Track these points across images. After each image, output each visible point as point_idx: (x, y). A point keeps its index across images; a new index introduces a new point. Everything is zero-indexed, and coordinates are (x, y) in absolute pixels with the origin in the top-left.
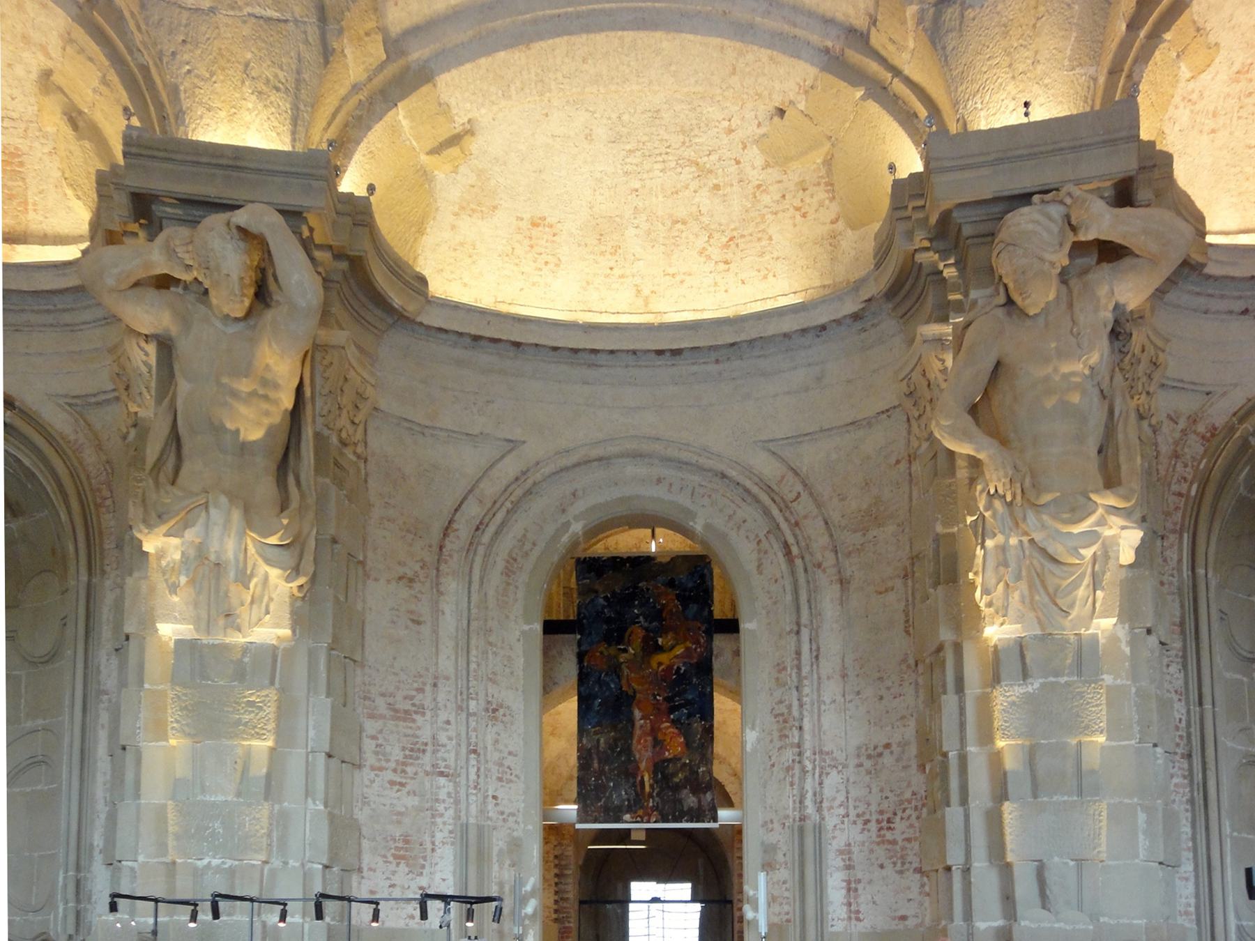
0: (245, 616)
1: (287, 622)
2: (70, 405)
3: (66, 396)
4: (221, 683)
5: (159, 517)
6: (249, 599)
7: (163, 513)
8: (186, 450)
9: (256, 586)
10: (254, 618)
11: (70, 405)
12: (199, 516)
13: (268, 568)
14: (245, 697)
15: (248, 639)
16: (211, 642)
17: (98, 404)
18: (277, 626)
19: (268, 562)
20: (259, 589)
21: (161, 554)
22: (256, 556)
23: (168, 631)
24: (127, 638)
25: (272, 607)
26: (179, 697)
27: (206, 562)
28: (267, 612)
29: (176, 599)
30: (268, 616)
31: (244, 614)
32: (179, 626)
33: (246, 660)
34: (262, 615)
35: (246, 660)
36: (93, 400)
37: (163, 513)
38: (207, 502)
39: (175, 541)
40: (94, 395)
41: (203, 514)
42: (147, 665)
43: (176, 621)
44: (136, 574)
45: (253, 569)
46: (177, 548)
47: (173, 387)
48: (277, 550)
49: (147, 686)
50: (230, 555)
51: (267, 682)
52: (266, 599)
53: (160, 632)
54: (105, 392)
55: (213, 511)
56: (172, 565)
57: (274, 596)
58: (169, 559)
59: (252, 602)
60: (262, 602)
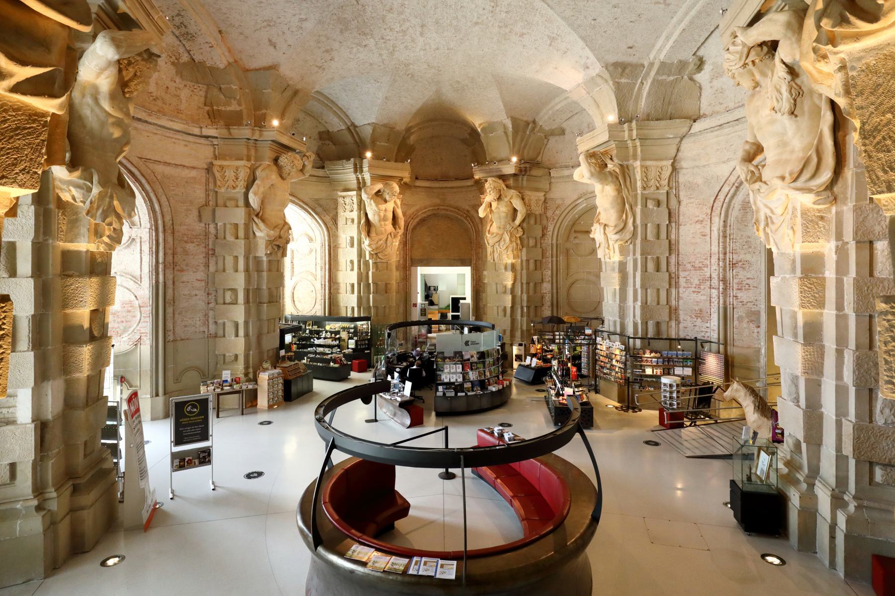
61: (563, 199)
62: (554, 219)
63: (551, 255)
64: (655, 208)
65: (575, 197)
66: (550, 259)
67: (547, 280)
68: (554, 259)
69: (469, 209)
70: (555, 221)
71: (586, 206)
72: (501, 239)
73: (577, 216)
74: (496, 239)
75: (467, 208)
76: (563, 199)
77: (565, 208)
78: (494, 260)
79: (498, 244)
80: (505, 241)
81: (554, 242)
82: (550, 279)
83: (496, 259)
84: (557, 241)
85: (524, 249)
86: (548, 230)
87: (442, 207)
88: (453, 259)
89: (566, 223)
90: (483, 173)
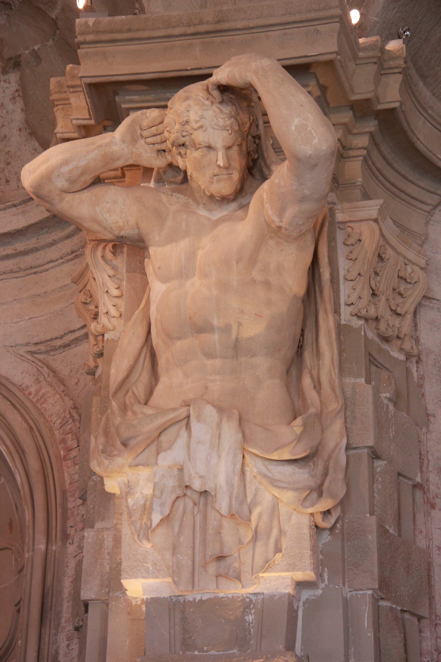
0: (247, 558)
1: (308, 561)
2: (32, 353)
3: (27, 344)
4: (213, 652)
5: (125, 444)
6: (250, 535)
7: (130, 438)
8: (162, 362)
9: (260, 516)
10: (259, 560)
11: (32, 353)
12: (177, 436)
13: (276, 492)
15: (252, 589)
16: (198, 598)
17: (66, 346)
18: (292, 567)
19: (273, 482)
20: (265, 518)
24: (86, 605)
25: (284, 544)
27: (189, 493)
28: (278, 550)
29: (147, 545)
30: (279, 556)
32: (151, 581)
33: (250, 618)
34: (271, 555)
35: (250, 618)
36: (59, 343)
37: (130, 438)
38: (188, 417)
40: (61, 337)
41: (184, 433)
42: (109, 640)
43: (147, 574)
44: (98, 525)
45: (255, 495)
47: (146, 296)
48: (288, 469)
50: (222, 480)
51: (281, 647)
52: (275, 532)
53: (130, 593)
54: (72, 332)
55: (194, 424)
56: (142, 502)
57: (286, 527)
58: (138, 495)
59: (255, 538)
60: (268, 537)
64: (391, 407)
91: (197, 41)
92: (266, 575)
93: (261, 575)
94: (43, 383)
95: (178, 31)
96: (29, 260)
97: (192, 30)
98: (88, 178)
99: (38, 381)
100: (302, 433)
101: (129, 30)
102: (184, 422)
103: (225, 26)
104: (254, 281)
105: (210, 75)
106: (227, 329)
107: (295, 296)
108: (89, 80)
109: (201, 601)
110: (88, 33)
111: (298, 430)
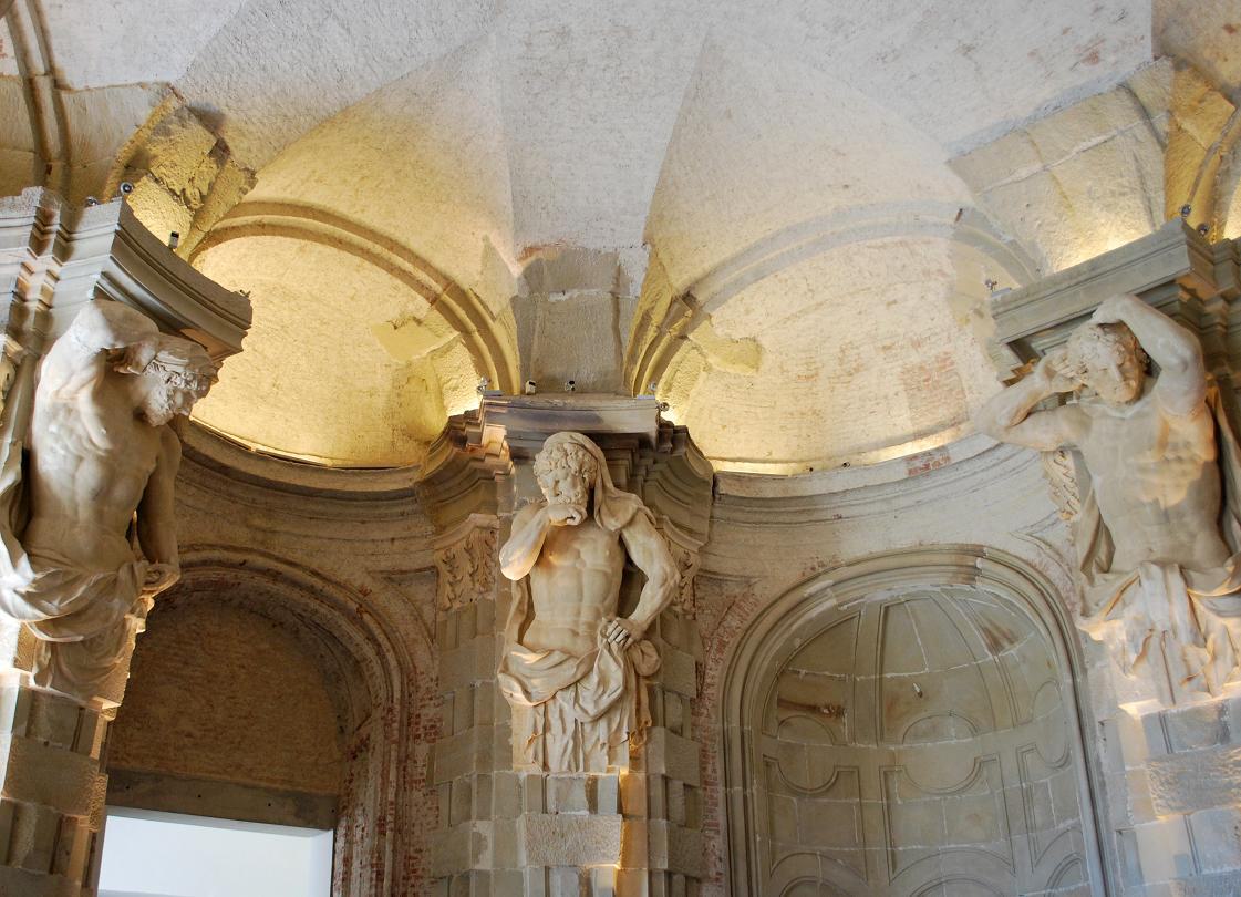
0: (1212, 675)
3: (1026, 527)
4: (1201, 749)
14: (1231, 757)
15: (1221, 697)
19: (1220, 613)
21: (1110, 637)
22: (1207, 612)
23: (1134, 709)
26: (1157, 773)
31: (1216, 673)
36: (1048, 522)
37: (1099, 601)
39: (1118, 624)
40: (1048, 518)
43: (1137, 698)
44: (1098, 664)
46: (1121, 629)
49: (1128, 768)
59: (1214, 658)
61: (748, 582)
62: (723, 644)
63: (720, 772)
65: (793, 576)
66: (721, 788)
67: (712, 873)
68: (738, 788)
69: (369, 584)
70: (728, 653)
71: (835, 608)
72: (586, 675)
73: (797, 642)
74: (569, 671)
75: (359, 579)
76: (748, 582)
77: (758, 610)
78: (545, 766)
79: (570, 694)
80: (603, 682)
81: (735, 724)
82: (722, 867)
83: (553, 764)
84: (742, 724)
85: (659, 733)
86: (708, 680)
87: (260, 561)
88: (267, 790)
89: (766, 664)
90: (522, 417)
91: (1078, 289)
92: (1230, 684)
93: (1226, 685)
94: (1043, 555)
95: (1063, 286)
96: (1011, 463)
97: (1074, 281)
98: (1023, 412)
99: (1039, 555)
100: (1234, 571)
101: (1028, 295)
102: (1137, 581)
103: (1099, 271)
104: (1167, 461)
105: (1089, 315)
106: (1156, 501)
107: (1206, 464)
108: (1008, 341)
109: (1183, 712)
110: (999, 307)
111: (1230, 569)
